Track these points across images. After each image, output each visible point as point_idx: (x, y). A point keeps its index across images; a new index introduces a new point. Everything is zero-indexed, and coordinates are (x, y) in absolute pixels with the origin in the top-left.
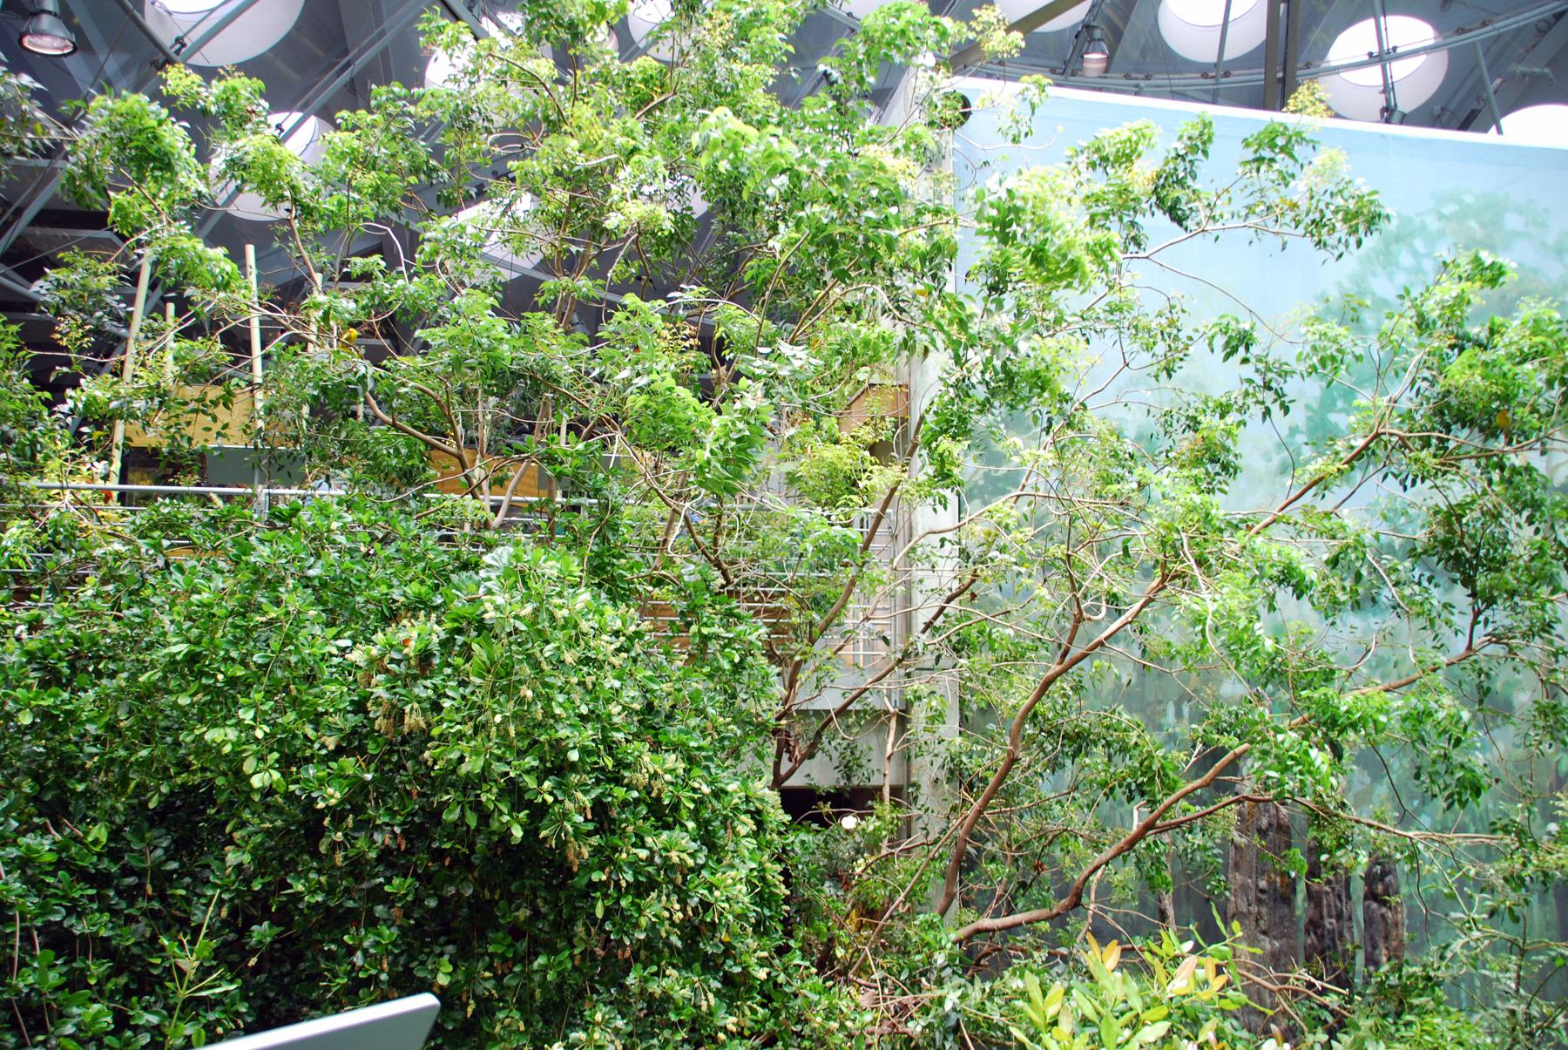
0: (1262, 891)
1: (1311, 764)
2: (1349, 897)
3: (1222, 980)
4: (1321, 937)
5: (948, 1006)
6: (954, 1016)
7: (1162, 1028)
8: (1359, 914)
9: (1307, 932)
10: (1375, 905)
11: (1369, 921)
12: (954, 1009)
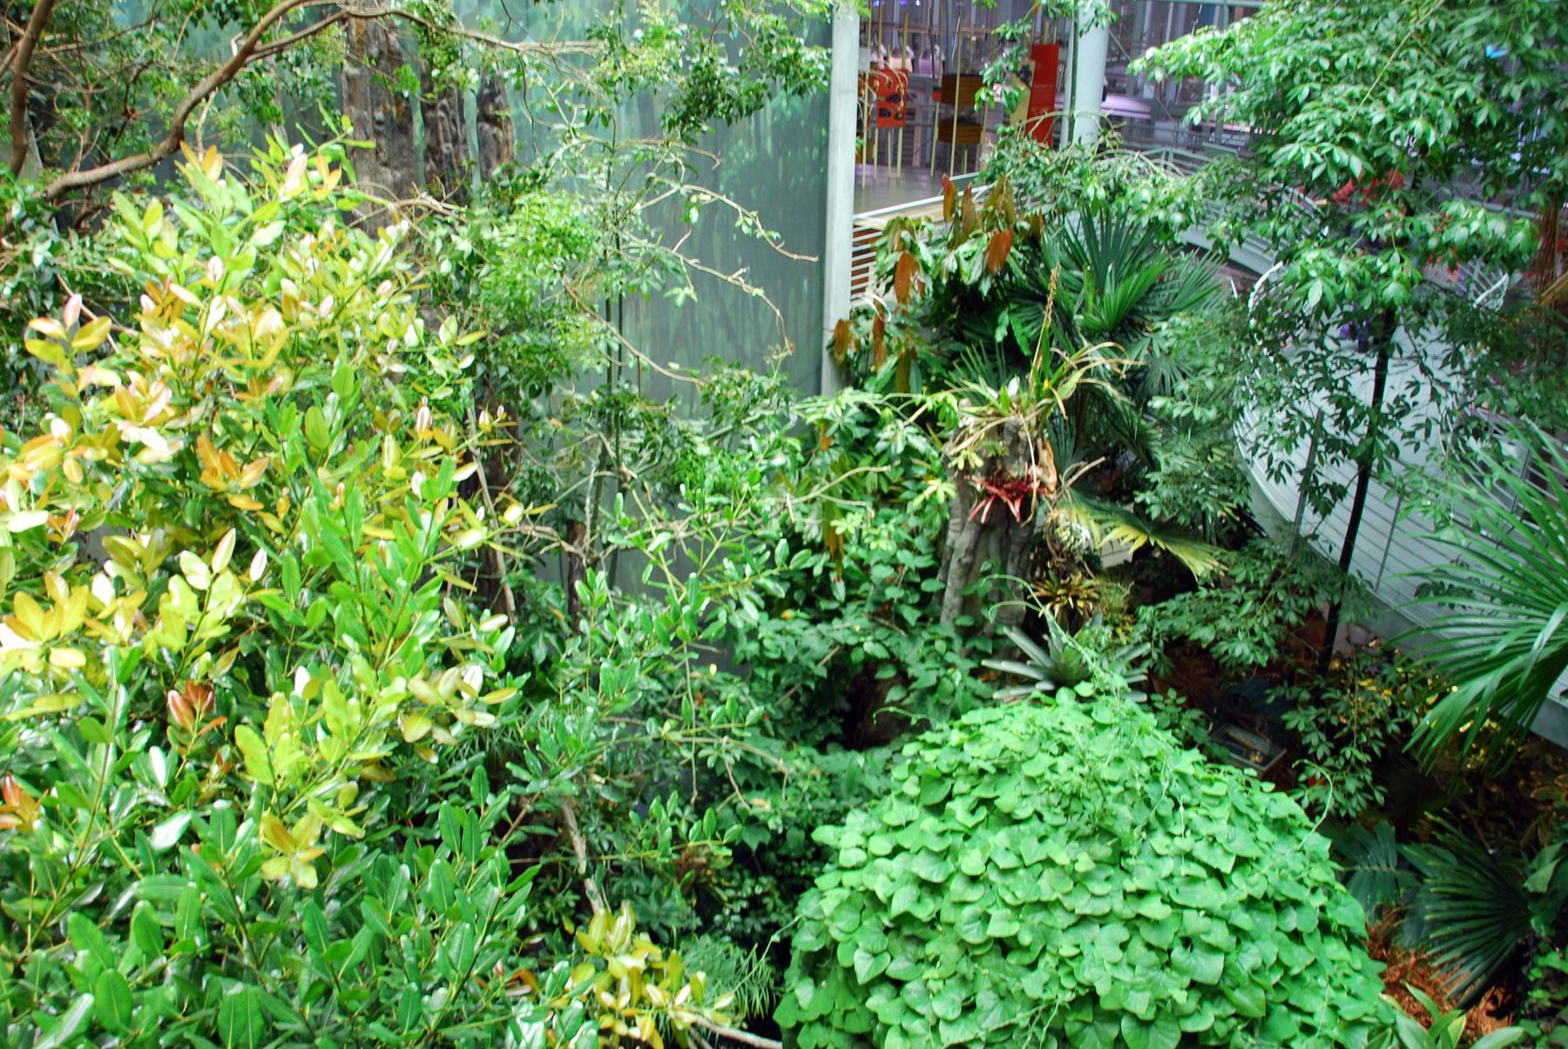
0: (379, 123)
2: (463, 121)
3: (337, 175)
4: (439, 163)
5: (38, 261)
6: (48, 273)
7: (277, 228)
10: (487, 126)
11: (483, 143)
12: (46, 263)
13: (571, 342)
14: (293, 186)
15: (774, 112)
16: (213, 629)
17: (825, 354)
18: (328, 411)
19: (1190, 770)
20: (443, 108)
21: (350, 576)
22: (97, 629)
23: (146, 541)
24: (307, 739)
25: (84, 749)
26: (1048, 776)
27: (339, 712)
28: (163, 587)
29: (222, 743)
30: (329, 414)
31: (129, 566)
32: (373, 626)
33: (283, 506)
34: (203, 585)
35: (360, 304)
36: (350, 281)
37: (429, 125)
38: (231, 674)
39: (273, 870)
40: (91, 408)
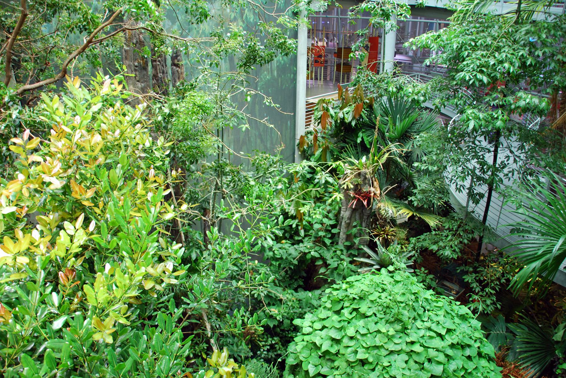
0: (136, 66)
1: (148, 6)
2: (166, 66)
3: (121, 86)
4: (157, 80)
5: (14, 117)
6: (18, 121)
7: (99, 105)
8: (170, 72)
9: (153, 79)
10: (175, 67)
11: (173, 73)
12: (17, 118)
13: (205, 144)
14: (106, 90)
15: (277, 62)
16: (76, 249)
17: (296, 148)
18: (117, 170)
19: (430, 297)
20: (159, 61)
21: (125, 230)
22: (33, 249)
23: (52, 217)
24: (110, 289)
25: (28, 293)
26: (378, 300)
27: (121, 279)
28: (58, 234)
29: (78, 290)
30: (118, 172)
31: (45, 226)
32: (134, 248)
33: (101, 205)
34: (72, 233)
35: (130, 132)
36: (126, 124)
37: (153, 66)
38: (82, 265)
39: (97, 337)
40: (33, 170)
